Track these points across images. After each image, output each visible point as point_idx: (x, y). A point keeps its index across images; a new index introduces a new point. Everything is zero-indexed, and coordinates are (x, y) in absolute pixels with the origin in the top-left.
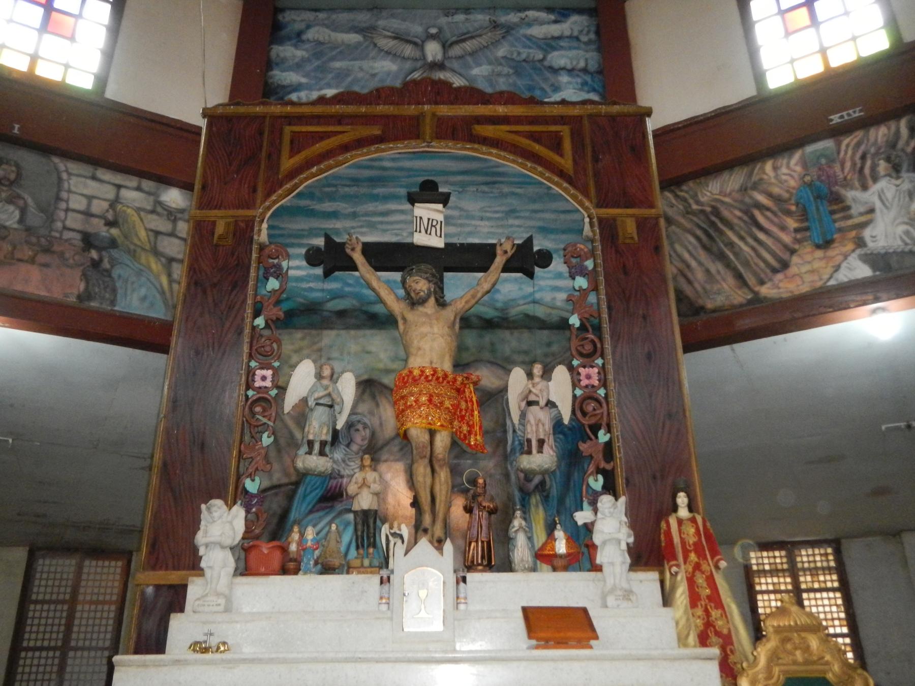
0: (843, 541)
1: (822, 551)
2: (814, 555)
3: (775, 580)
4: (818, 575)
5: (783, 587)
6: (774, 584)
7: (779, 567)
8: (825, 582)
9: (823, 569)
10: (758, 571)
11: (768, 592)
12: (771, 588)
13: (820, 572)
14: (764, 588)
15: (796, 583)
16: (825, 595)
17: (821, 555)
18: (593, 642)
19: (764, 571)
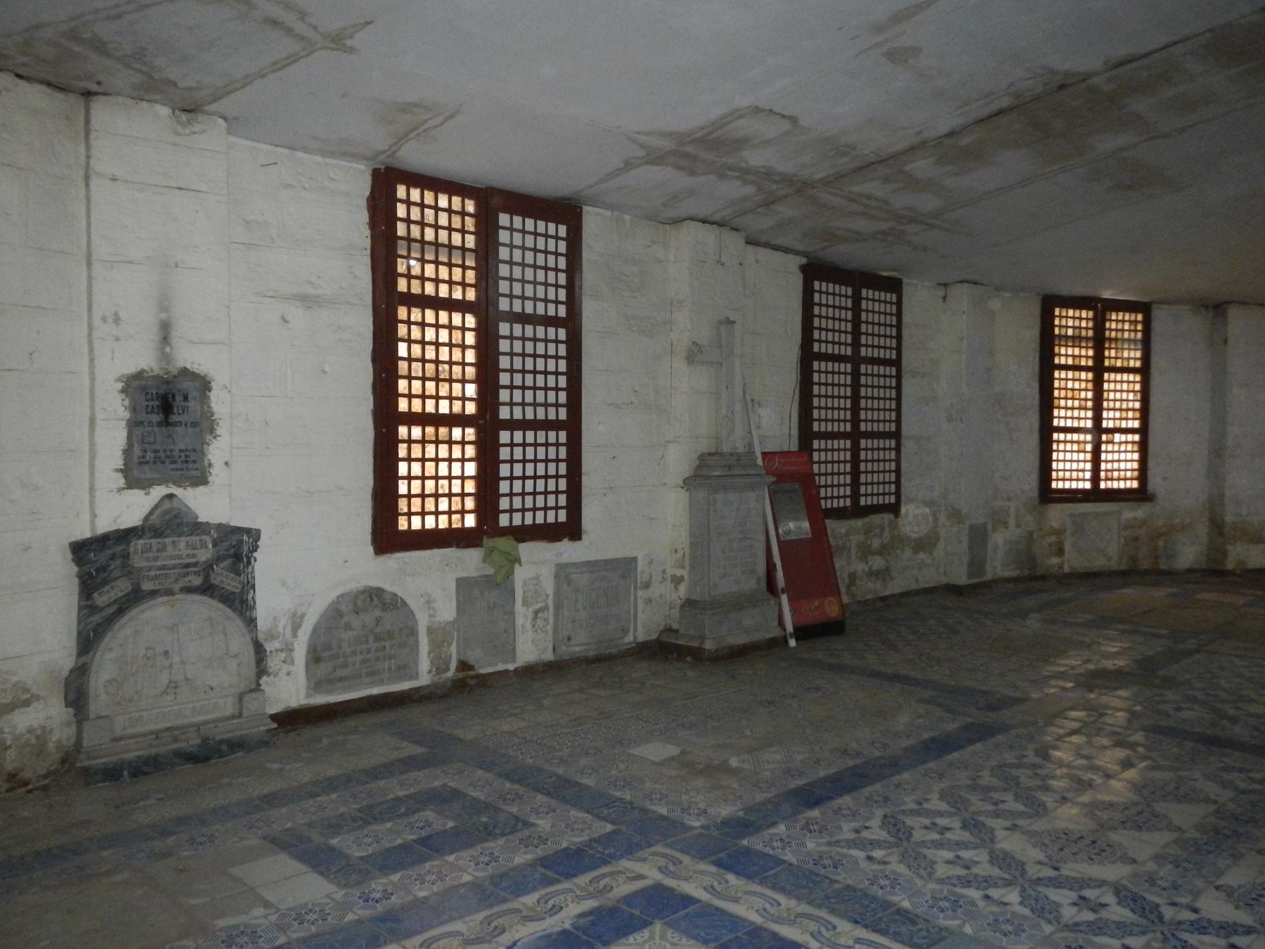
0: (1154, 306)
1: (1133, 318)
2: (1123, 321)
3: (1077, 351)
4: (1123, 349)
5: (1083, 363)
6: (1074, 356)
7: (1084, 333)
8: (1129, 359)
9: (1129, 340)
10: (1060, 336)
11: (1066, 368)
12: (1070, 362)
13: (1126, 346)
14: (1063, 361)
15: (1099, 357)
16: (1125, 377)
17: (1130, 322)
18: (120, 386)
19: (1066, 337)
